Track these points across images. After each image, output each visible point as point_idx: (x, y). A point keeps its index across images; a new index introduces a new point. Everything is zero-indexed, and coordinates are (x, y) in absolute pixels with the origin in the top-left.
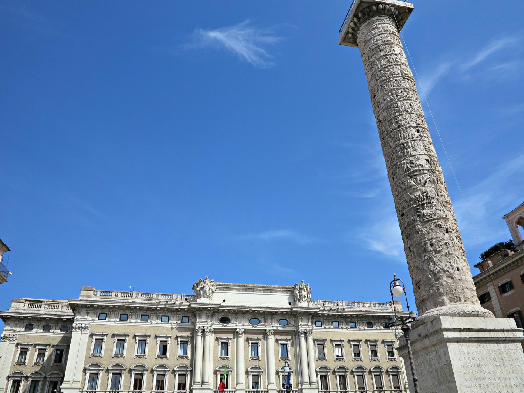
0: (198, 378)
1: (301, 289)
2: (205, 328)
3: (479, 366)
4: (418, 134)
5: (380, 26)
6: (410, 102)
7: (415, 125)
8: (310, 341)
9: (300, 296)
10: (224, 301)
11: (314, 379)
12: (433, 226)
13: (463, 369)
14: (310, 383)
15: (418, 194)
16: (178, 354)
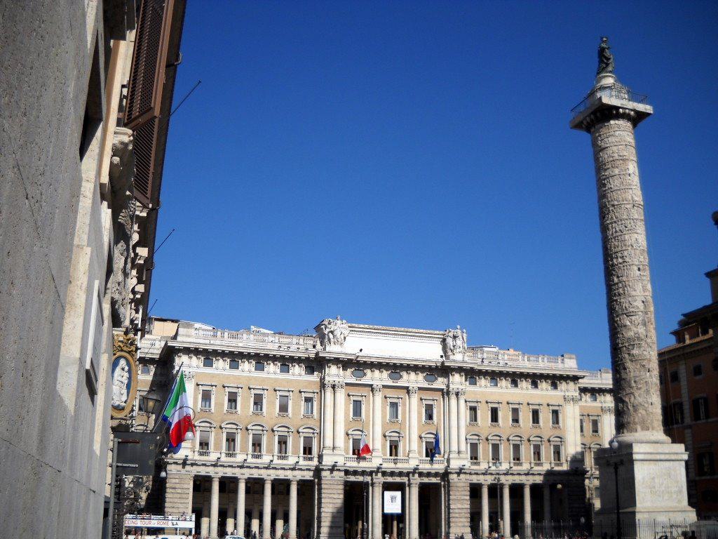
0: (329, 442)
1: (455, 337)
2: (336, 383)
3: (653, 478)
4: (638, 273)
5: (617, 133)
6: (636, 235)
7: (637, 263)
8: (462, 402)
9: (454, 346)
10: (361, 350)
11: (463, 448)
12: (639, 366)
13: (642, 481)
14: (459, 452)
15: (632, 334)
16: (302, 413)
